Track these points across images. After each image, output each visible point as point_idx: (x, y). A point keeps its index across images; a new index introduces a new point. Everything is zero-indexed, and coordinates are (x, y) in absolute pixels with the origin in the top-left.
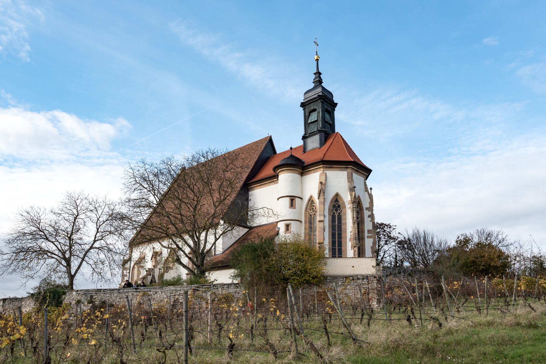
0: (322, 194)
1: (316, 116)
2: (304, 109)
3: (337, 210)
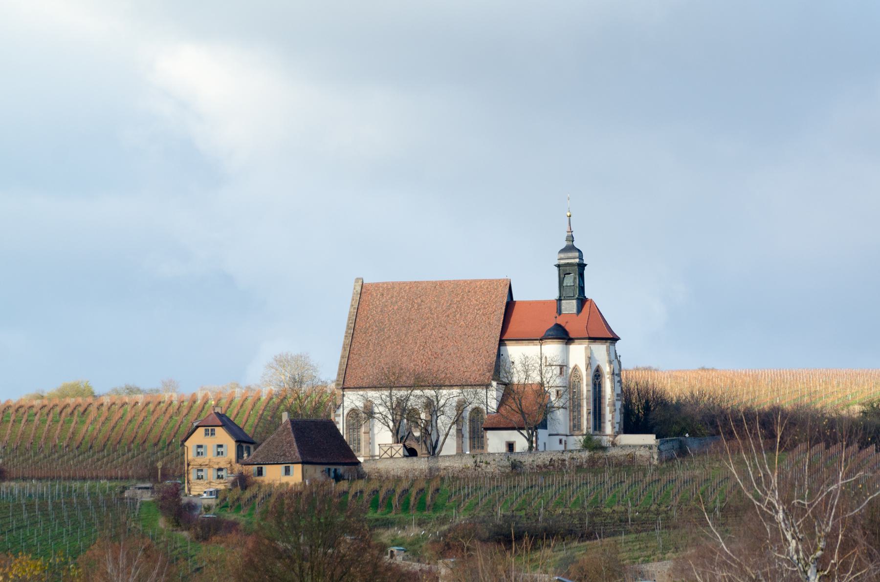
0: (589, 367)
1: (572, 280)
2: (559, 270)
3: (597, 379)
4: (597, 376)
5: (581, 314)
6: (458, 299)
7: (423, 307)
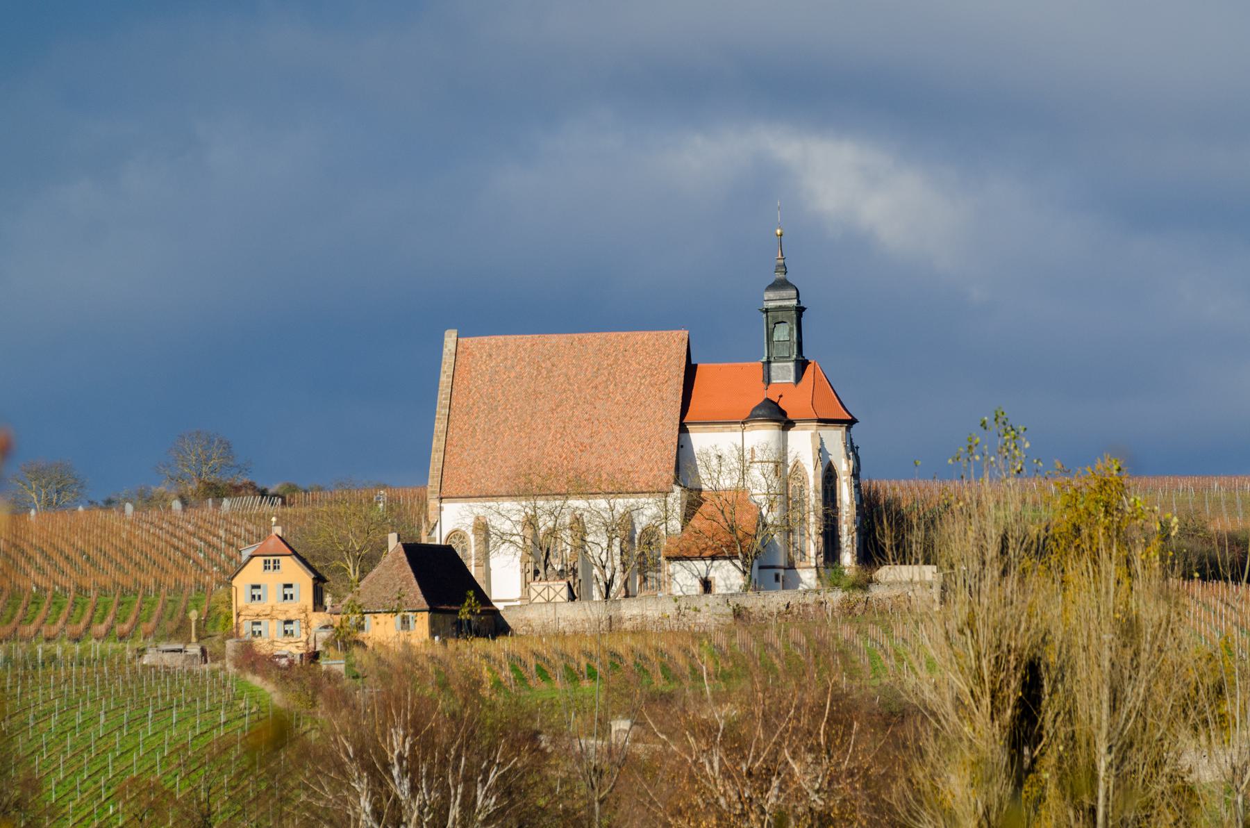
1: (786, 332)
4: (829, 477)
5: (800, 384)
7: (556, 374)
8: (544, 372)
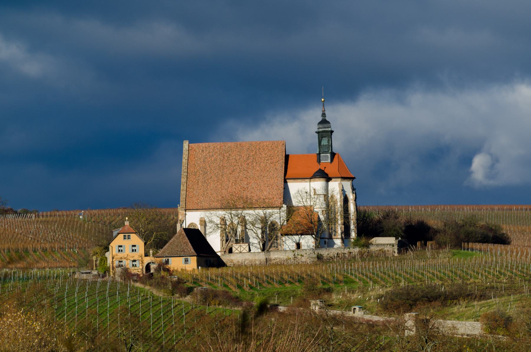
1: (326, 141)
2: (319, 135)
4: (346, 200)
5: (333, 163)
6: (253, 154)
8: (226, 158)
